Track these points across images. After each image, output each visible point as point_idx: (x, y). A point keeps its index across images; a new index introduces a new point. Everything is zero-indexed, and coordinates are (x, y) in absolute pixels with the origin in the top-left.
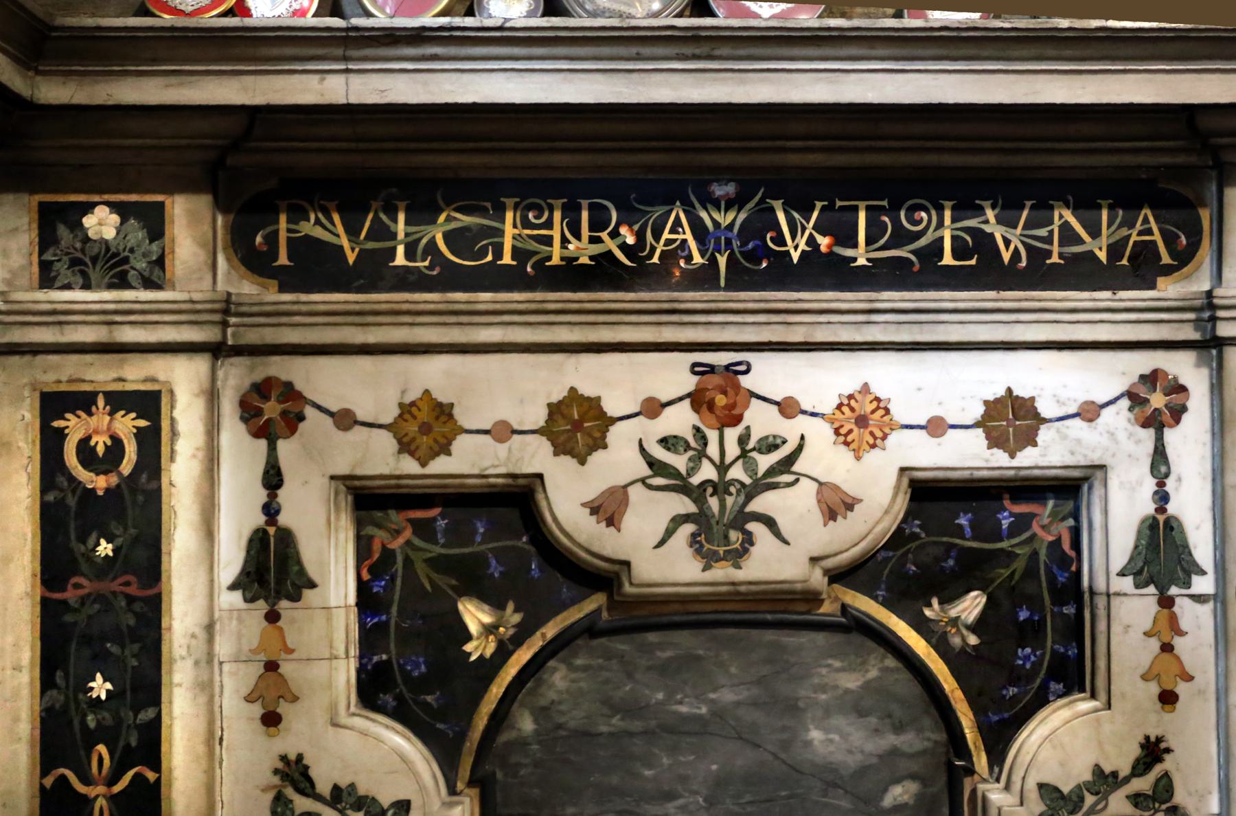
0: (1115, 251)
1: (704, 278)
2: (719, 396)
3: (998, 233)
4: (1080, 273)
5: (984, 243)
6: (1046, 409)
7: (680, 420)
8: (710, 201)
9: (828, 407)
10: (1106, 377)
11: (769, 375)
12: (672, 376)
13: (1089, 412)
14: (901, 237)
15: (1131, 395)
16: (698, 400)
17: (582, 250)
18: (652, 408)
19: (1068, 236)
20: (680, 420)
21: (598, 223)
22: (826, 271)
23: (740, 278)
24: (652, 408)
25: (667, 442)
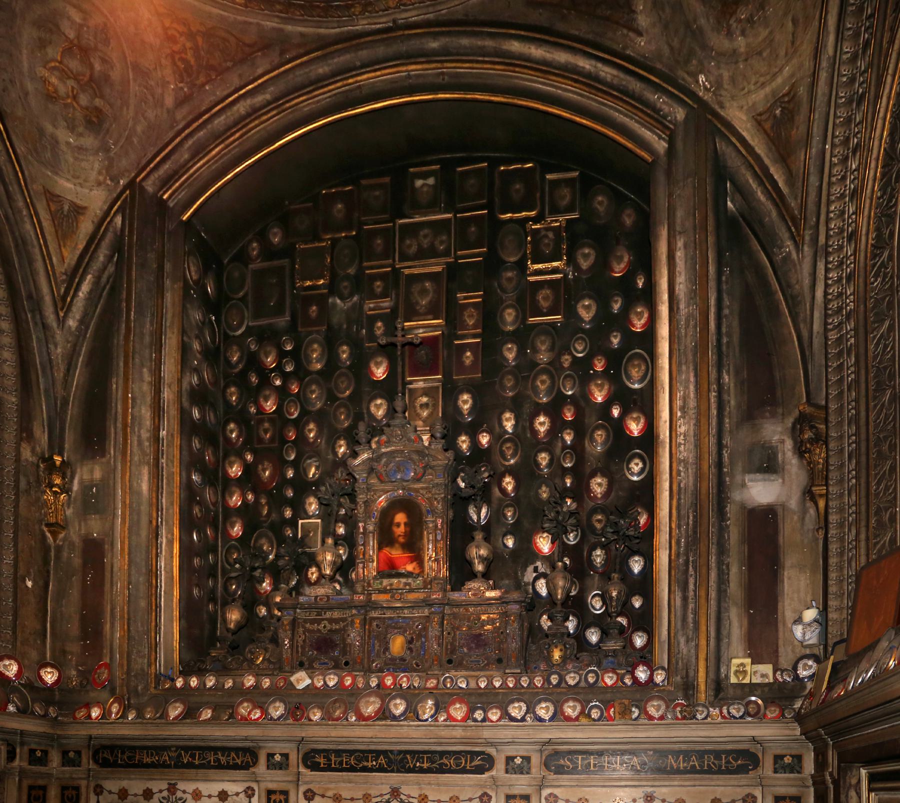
0: (242, 762)
1: (169, 766)
2: (172, 789)
3: (221, 758)
4: (236, 767)
5: (219, 760)
6: (230, 793)
7: (165, 794)
8: (171, 751)
9: (191, 791)
10: (239, 788)
11: (181, 786)
12: (164, 785)
13: (237, 794)
14: (204, 759)
15: (245, 791)
16: (168, 790)
17: (149, 760)
18: (161, 791)
19: (234, 759)
20: (165, 794)
21: (152, 755)
22: (190, 766)
23: (176, 766)
24: (161, 791)
25: (163, 798)
